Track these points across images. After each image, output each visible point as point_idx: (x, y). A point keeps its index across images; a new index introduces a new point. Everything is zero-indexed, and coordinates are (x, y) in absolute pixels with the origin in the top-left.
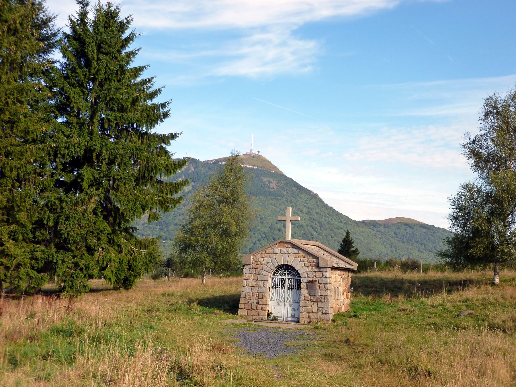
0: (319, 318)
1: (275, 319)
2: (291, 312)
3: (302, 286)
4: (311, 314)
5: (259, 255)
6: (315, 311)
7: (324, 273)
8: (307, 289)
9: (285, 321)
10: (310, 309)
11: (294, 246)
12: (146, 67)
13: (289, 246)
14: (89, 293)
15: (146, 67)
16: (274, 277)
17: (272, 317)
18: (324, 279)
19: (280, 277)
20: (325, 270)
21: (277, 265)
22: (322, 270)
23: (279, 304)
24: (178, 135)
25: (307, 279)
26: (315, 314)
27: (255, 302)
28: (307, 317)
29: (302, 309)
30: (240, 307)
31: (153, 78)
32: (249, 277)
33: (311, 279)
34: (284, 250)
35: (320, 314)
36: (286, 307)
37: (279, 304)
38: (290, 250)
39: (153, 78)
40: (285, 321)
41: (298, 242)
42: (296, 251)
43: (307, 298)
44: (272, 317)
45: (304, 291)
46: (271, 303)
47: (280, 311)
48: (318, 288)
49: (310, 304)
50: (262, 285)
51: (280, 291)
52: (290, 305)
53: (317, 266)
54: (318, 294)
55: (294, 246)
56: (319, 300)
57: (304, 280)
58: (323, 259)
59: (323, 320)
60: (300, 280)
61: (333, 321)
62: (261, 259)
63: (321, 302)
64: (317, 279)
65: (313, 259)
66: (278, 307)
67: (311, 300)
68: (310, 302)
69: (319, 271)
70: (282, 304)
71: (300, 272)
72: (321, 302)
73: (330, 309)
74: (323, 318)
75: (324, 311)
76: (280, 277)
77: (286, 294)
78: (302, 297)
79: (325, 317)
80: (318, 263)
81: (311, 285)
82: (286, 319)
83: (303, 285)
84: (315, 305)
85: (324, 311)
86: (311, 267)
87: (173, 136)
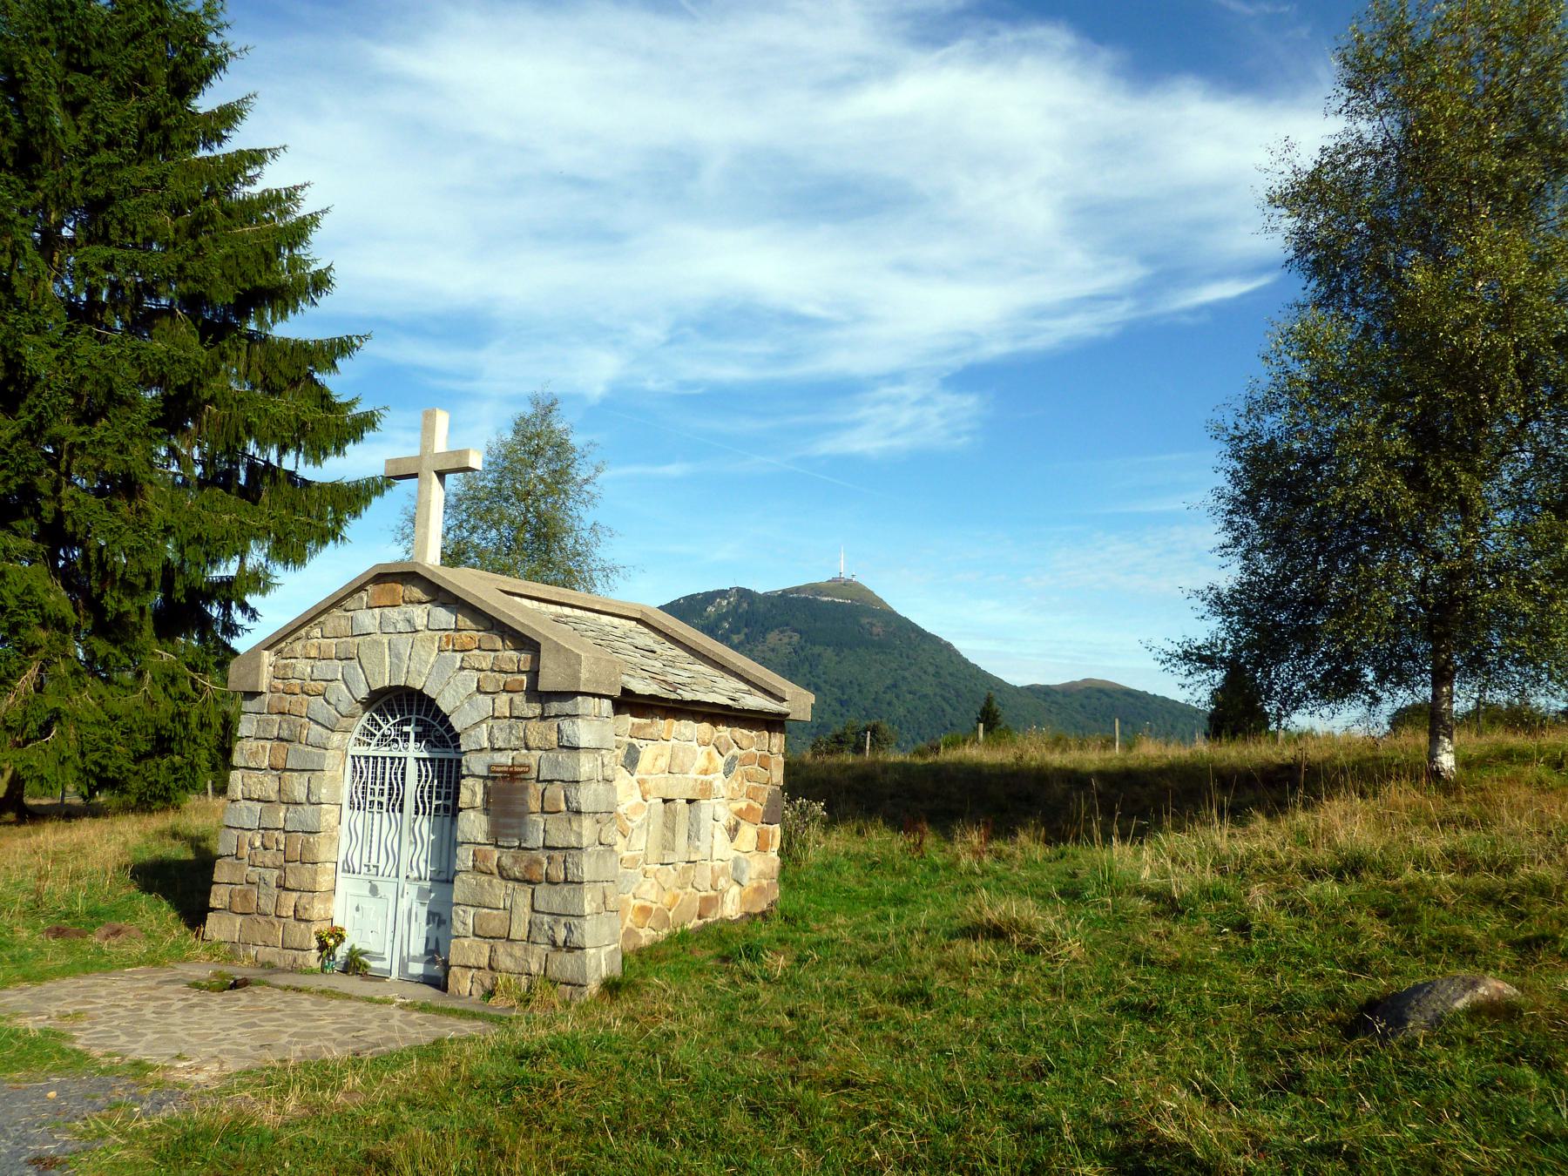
0: (534, 968)
1: (355, 965)
2: (424, 928)
3: (464, 797)
4: (501, 947)
5: (298, 646)
6: (519, 931)
7: (566, 725)
8: (486, 811)
9: (395, 975)
10: (495, 925)
11: (439, 595)
12: (274, 152)
13: (417, 593)
14: (15, 829)
15: (274, 152)
16: (363, 751)
17: (341, 952)
18: (562, 756)
19: (384, 751)
20: (567, 707)
21: (363, 693)
22: (554, 707)
23: (374, 891)
24: (356, 342)
25: (487, 757)
26: (517, 951)
27: (272, 876)
28: (484, 962)
29: (464, 919)
30: (213, 903)
31: (302, 187)
32: (254, 754)
33: (505, 759)
34: (392, 613)
35: (543, 948)
36: (404, 904)
37: (374, 891)
38: (419, 614)
39: (302, 187)
40: (395, 975)
41: (471, 582)
42: (444, 617)
43: (486, 858)
44: (341, 952)
45: (473, 824)
46: (345, 883)
47: (380, 928)
48: (534, 805)
49: (499, 891)
50: (300, 793)
51: (383, 824)
52: (422, 894)
53: (535, 693)
54: (536, 839)
55: (439, 595)
56: (539, 873)
57: (476, 764)
58: (558, 648)
59: (554, 983)
60: (459, 761)
61: (612, 988)
62: (303, 666)
63: (551, 882)
64: (532, 758)
65: (514, 655)
66: (369, 904)
67: (504, 874)
68: (496, 881)
69: (543, 717)
70: (387, 888)
71: (457, 723)
72: (551, 882)
73: (589, 926)
74: (554, 971)
75: (561, 935)
76: (384, 751)
77: (406, 838)
78: (465, 857)
79: (564, 964)
80: (534, 674)
81: (506, 791)
82: (403, 966)
83: (471, 792)
84: (523, 898)
85: (561, 935)
86: (505, 697)
87: (343, 347)
